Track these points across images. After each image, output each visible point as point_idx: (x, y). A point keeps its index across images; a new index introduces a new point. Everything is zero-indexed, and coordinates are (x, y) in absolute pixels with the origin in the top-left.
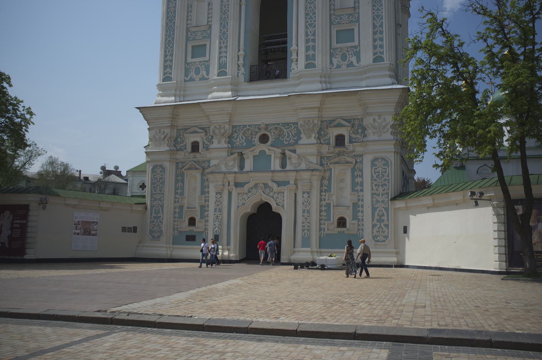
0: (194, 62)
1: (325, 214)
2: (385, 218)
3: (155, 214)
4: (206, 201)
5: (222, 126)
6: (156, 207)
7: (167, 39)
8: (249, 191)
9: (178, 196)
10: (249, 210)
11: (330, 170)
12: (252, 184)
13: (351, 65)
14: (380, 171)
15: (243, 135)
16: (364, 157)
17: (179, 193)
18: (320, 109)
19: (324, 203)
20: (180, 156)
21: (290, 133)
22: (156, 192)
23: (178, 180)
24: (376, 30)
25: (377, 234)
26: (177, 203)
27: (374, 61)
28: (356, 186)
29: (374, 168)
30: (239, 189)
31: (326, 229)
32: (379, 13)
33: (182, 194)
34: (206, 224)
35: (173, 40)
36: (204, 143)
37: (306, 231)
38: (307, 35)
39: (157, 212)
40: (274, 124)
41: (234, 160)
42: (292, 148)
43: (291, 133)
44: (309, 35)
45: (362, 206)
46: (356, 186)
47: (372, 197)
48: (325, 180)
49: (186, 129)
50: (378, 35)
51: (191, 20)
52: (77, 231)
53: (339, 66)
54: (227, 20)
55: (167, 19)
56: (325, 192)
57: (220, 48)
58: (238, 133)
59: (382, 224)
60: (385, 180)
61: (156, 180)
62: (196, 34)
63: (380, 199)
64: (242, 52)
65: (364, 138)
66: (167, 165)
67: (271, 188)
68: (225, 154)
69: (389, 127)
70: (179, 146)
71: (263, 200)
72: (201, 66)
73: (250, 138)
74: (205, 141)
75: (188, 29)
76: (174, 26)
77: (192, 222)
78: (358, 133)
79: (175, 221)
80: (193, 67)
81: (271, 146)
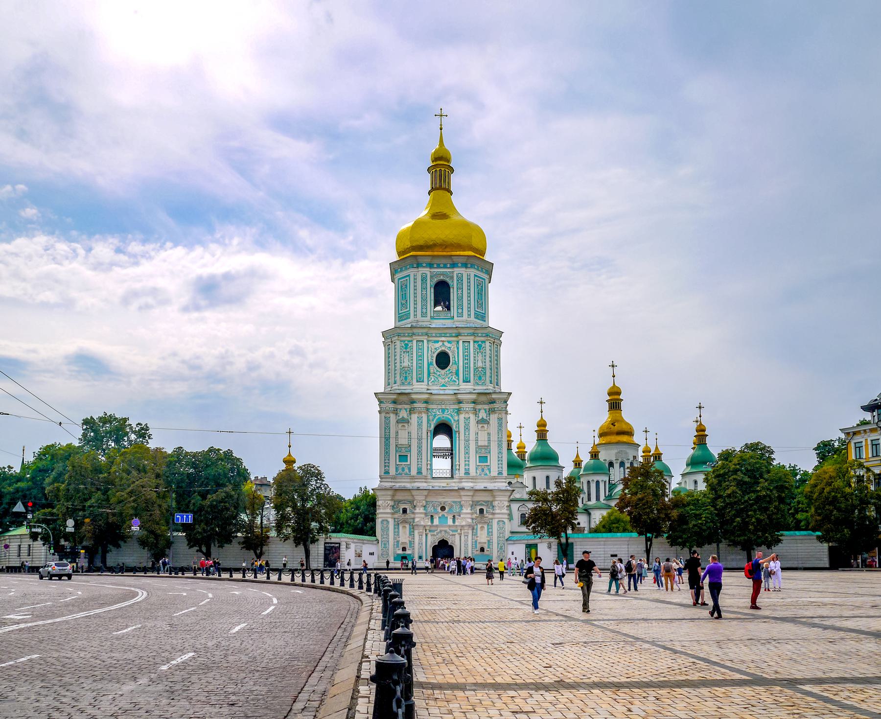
11: (477, 525)
12: (439, 530)
13: (486, 474)
18: (472, 496)
19: (474, 541)
20: (396, 516)
28: (490, 533)
33: (398, 535)
38: (465, 458)
39: (385, 544)
46: (490, 533)
49: (400, 501)
53: (480, 475)
57: (418, 459)
63: (501, 539)
66: (390, 520)
75: (396, 445)
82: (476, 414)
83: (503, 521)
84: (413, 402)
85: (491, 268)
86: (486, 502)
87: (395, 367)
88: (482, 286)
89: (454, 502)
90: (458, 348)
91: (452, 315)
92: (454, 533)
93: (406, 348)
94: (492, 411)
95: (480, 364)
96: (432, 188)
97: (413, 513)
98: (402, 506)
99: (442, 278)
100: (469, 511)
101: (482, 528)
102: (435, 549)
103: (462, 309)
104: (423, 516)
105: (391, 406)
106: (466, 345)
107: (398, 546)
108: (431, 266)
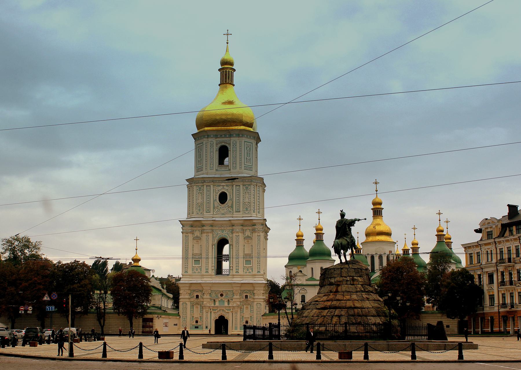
2: (260, 321)
4: (202, 315)
10: (217, 318)
11: (243, 306)
13: (250, 272)
20: (192, 300)
33: (193, 312)
34: (202, 322)
36: (201, 295)
38: (236, 262)
39: (184, 318)
40: (226, 291)
41: (212, 302)
42: (231, 299)
52: (164, 326)
53: (246, 273)
57: (206, 263)
64: (213, 265)
69: (261, 294)
77: (197, 322)
82: (244, 233)
84: (203, 226)
85: (257, 136)
86: (249, 291)
87: (193, 203)
88: (250, 148)
90: (233, 190)
91: (230, 168)
92: (228, 311)
93: (200, 191)
94: (254, 231)
95: (247, 200)
96: (221, 82)
97: (203, 298)
99: (223, 144)
100: (238, 297)
101: (247, 308)
102: (217, 322)
103: (236, 164)
104: (209, 300)
105: (189, 229)
106: (238, 188)
107: (193, 320)
108: (216, 136)
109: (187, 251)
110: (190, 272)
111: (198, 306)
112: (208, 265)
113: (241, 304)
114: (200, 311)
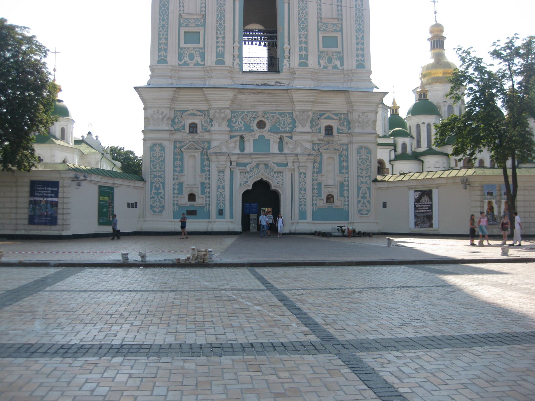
0: (188, 48)
1: (317, 192)
2: (367, 195)
3: (155, 190)
4: (206, 179)
5: (223, 111)
6: (156, 184)
7: (160, 22)
8: (251, 171)
9: (176, 173)
11: (321, 155)
12: (254, 164)
13: (335, 67)
14: (364, 158)
15: (242, 120)
16: (349, 145)
17: (178, 171)
18: (314, 102)
19: (316, 182)
20: (178, 136)
21: (286, 121)
22: (156, 170)
23: (177, 158)
24: (358, 41)
25: (362, 208)
26: (176, 181)
27: (357, 67)
28: (343, 169)
29: (359, 155)
30: (240, 168)
31: (318, 205)
32: (359, 27)
33: (182, 171)
34: (208, 199)
35: (167, 24)
36: (202, 125)
37: (303, 206)
38: (300, 37)
39: (157, 189)
41: (235, 142)
42: (289, 135)
43: (287, 121)
44: (302, 38)
45: (348, 186)
46: (343, 169)
47: (358, 179)
48: (317, 164)
50: (360, 45)
51: (183, 7)
53: (325, 67)
54: (223, 13)
55: (160, 3)
56: (317, 173)
57: (217, 38)
58: (236, 118)
59: (365, 201)
60: (368, 165)
61: (155, 158)
62: (188, 21)
63: (364, 180)
65: (348, 130)
66: (166, 144)
67: (271, 168)
68: (226, 136)
70: (177, 126)
71: (264, 179)
72: (195, 52)
73: (248, 123)
74: (203, 123)
75: (180, 15)
76: (168, 10)
77: (192, 197)
78: (343, 126)
79: (174, 197)
80: (186, 52)
81: (269, 131)
83: (367, 148)
86: (336, 115)
89: (282, 113)
98: (189, 120)
102: (247, 196)
109: (164, 5)
110: (172, 59)
111: (196, 154)
112: (224, 43)
113: (313, 149)
114: (203, 166)
